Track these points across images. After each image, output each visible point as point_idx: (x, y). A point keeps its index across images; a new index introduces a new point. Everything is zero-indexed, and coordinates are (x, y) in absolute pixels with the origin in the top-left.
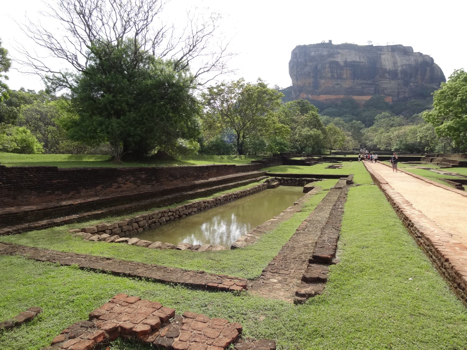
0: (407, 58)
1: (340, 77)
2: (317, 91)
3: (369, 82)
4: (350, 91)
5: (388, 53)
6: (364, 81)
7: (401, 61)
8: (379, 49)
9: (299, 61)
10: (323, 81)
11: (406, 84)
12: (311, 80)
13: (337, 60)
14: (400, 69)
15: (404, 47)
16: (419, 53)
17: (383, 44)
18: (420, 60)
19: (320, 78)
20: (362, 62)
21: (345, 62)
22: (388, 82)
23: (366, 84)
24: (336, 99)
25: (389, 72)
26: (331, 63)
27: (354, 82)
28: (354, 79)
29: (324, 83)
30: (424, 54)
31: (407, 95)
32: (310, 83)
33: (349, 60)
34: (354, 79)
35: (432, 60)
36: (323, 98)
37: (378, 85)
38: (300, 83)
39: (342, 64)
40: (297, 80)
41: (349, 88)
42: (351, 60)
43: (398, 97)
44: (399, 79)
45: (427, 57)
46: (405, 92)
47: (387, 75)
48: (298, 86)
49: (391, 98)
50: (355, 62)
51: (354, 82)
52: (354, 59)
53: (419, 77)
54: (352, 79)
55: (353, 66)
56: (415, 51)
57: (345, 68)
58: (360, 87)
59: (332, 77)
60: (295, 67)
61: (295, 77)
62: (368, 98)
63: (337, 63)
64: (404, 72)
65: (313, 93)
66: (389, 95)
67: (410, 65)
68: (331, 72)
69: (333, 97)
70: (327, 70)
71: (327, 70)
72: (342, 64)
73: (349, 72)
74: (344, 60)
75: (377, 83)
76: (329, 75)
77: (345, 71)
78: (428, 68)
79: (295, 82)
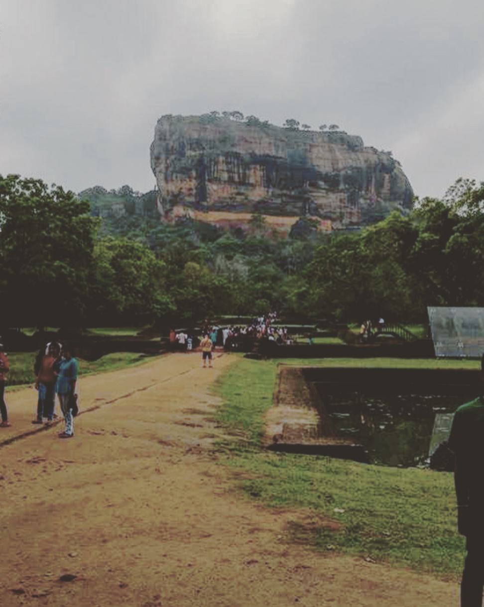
0: (353, 156)
1: (243, 182)
2: (205, 203)
3: (293, 193)
4: (262, 207)
5: (323, 144)
6: (285, 192)
7: (345, 161)
8: (308, 134)
9: (170, 147)
10: (215, 187)
11: (353, 200)
12: (193, 183)
13: (238, 151)
14: (343, 173)
15: (349, 136)
16: (372, 148)
17: (315, 128)
18: (374, 159)
19: (210, 181)
20: (281, 158)
21: (253, 155)
22: (325, 195)
23: (291, 197)
24: (239, 220)
25: (326, 178)
26: (227, 155)
27: (268, 192)
28: (268, 187)
29: (215, 191)
30: (380, 150)
31: (355, 220)
32: (190, 189)
33: (257, 152)
34: (268, 187)
35: (393, 162)
36: (213, 217)
37: (309, 199)
38: (173, 187)
39: (247, 158)
40: (166, 180)
41: (259, 202)
42: (262, 153)
43: (341, 221)
44: (342, 191)
45: (384, 158)
46: (351, 213)
47: (321, 183)
48: (168, 191)
49: (329, 222)
50: (268, 156)
51: (268, 192)
52: (267, 152)
53: (373, 190)
54: (264, 187)
55: (265, 162)
56: (367, 143)
57: (252, 166)
58: (279, 201)
59: (231, 181)
60: (163, 157)
61: (162, 176)
62: (293, 220)
63: (237, 156)
64: (348, 179)
65: (197, 206)
66: (326, 217)
67: (359, 170)
68: (229, 171)
69: (232, 216)
70: (220, 167)
71: (220, 167)
72: (247, 158)
73: (259, 173)
74: (250, 151)
75: (306, 196)
76: (225, 176)
77: (252, 171)
78: (387, 177)
79: (163, 184)
